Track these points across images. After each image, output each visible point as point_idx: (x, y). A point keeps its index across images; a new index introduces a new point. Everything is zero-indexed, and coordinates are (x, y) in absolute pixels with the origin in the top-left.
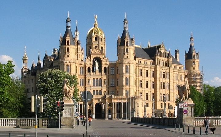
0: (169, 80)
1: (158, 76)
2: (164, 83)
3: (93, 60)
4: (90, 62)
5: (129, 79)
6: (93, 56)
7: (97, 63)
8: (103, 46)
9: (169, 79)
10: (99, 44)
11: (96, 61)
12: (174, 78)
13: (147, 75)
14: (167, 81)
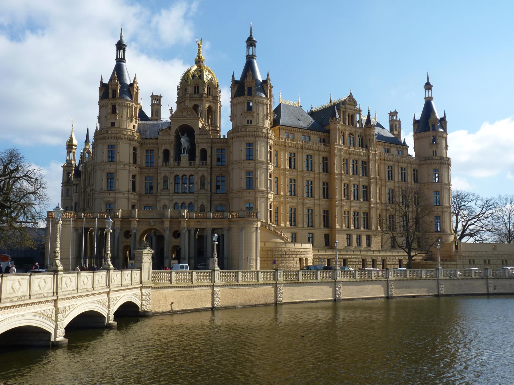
3: (177, 132)
4: (168, 137)
7: (183, 140)
8: (212, 105)
9: (369, 176)
10: (202, 100)
11: (183, 135)
12: (385, 175)
13: (310, 167)
14: (363, 181)
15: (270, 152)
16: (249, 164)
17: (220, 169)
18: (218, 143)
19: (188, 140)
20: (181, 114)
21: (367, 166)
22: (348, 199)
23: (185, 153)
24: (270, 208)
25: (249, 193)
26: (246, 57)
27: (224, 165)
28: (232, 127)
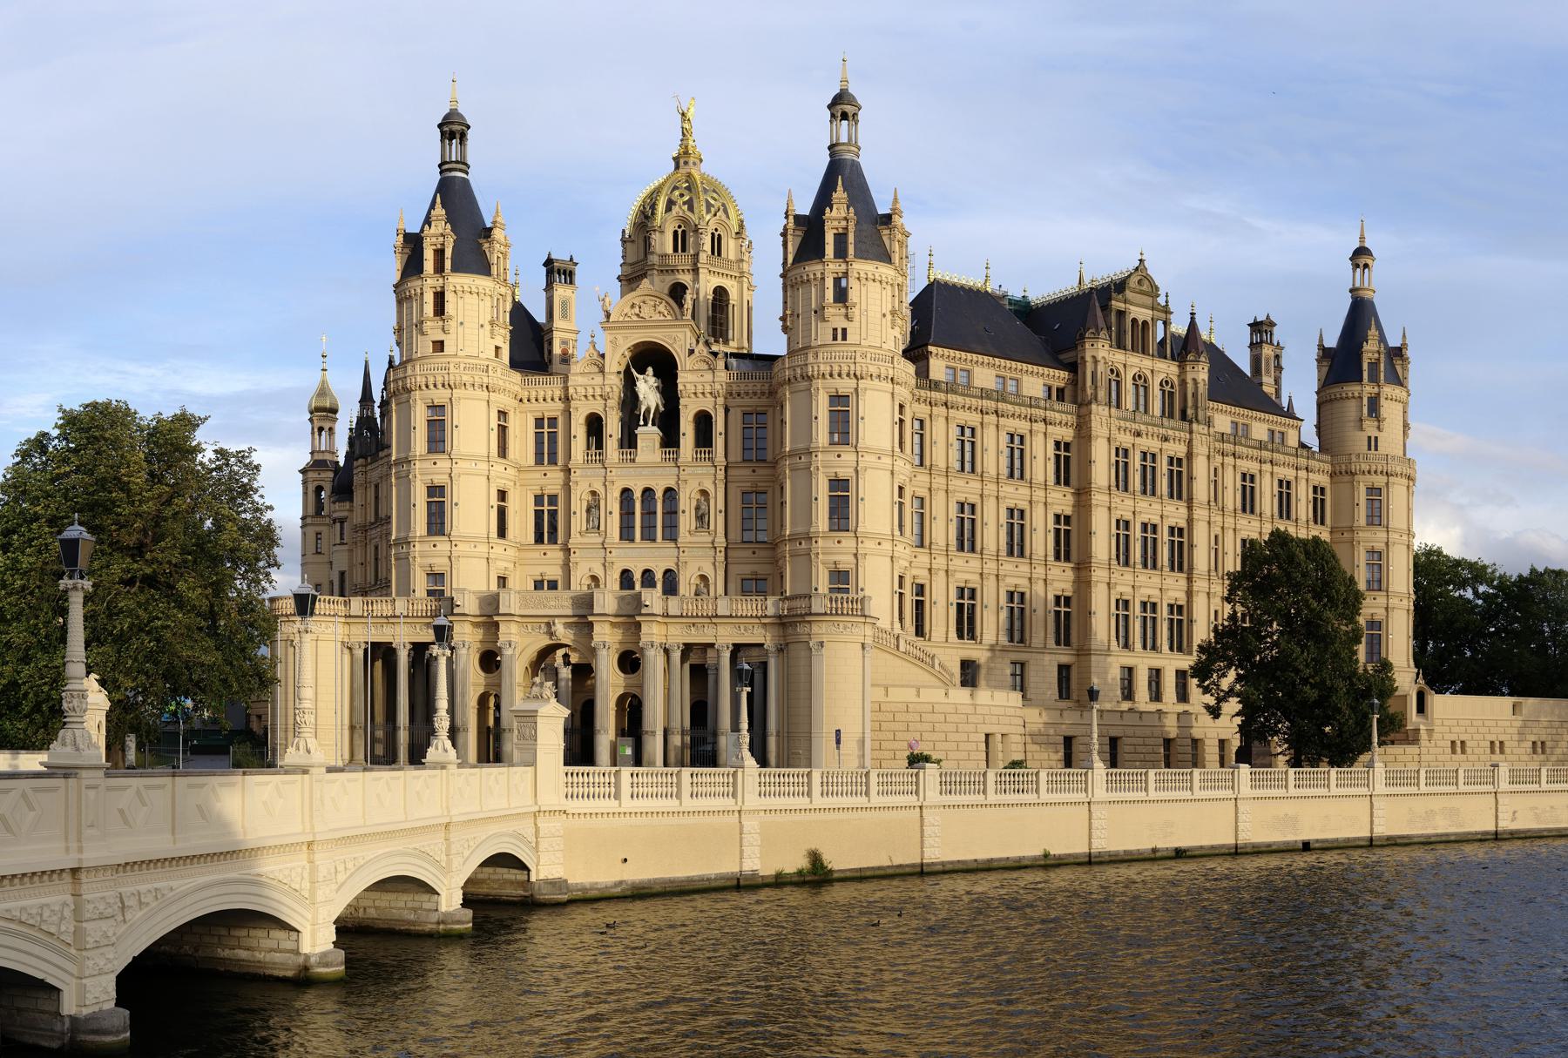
0: (1190, 508)
1: (1101, 473)
2: (1145, 526)
4: (598, 379)
5: (852, 485)
6: (620, 340)
9: (1190, 500)
11: (642, 371)
12: (1232, 498)
13: (1017, 469)
14: (1175, 514)
15: (901, 421)
16: (839, 456)
17: (754, 471)
18: (747, 394)
19: (657, 387)
20: (637, 310)
21: (1184, 469)
22: (1127, 564)
23: (650, 424)
24: (901, 587)
25: (839, 542)
26: (829, 148)
27: (764, 461)
28: (788, 350)
